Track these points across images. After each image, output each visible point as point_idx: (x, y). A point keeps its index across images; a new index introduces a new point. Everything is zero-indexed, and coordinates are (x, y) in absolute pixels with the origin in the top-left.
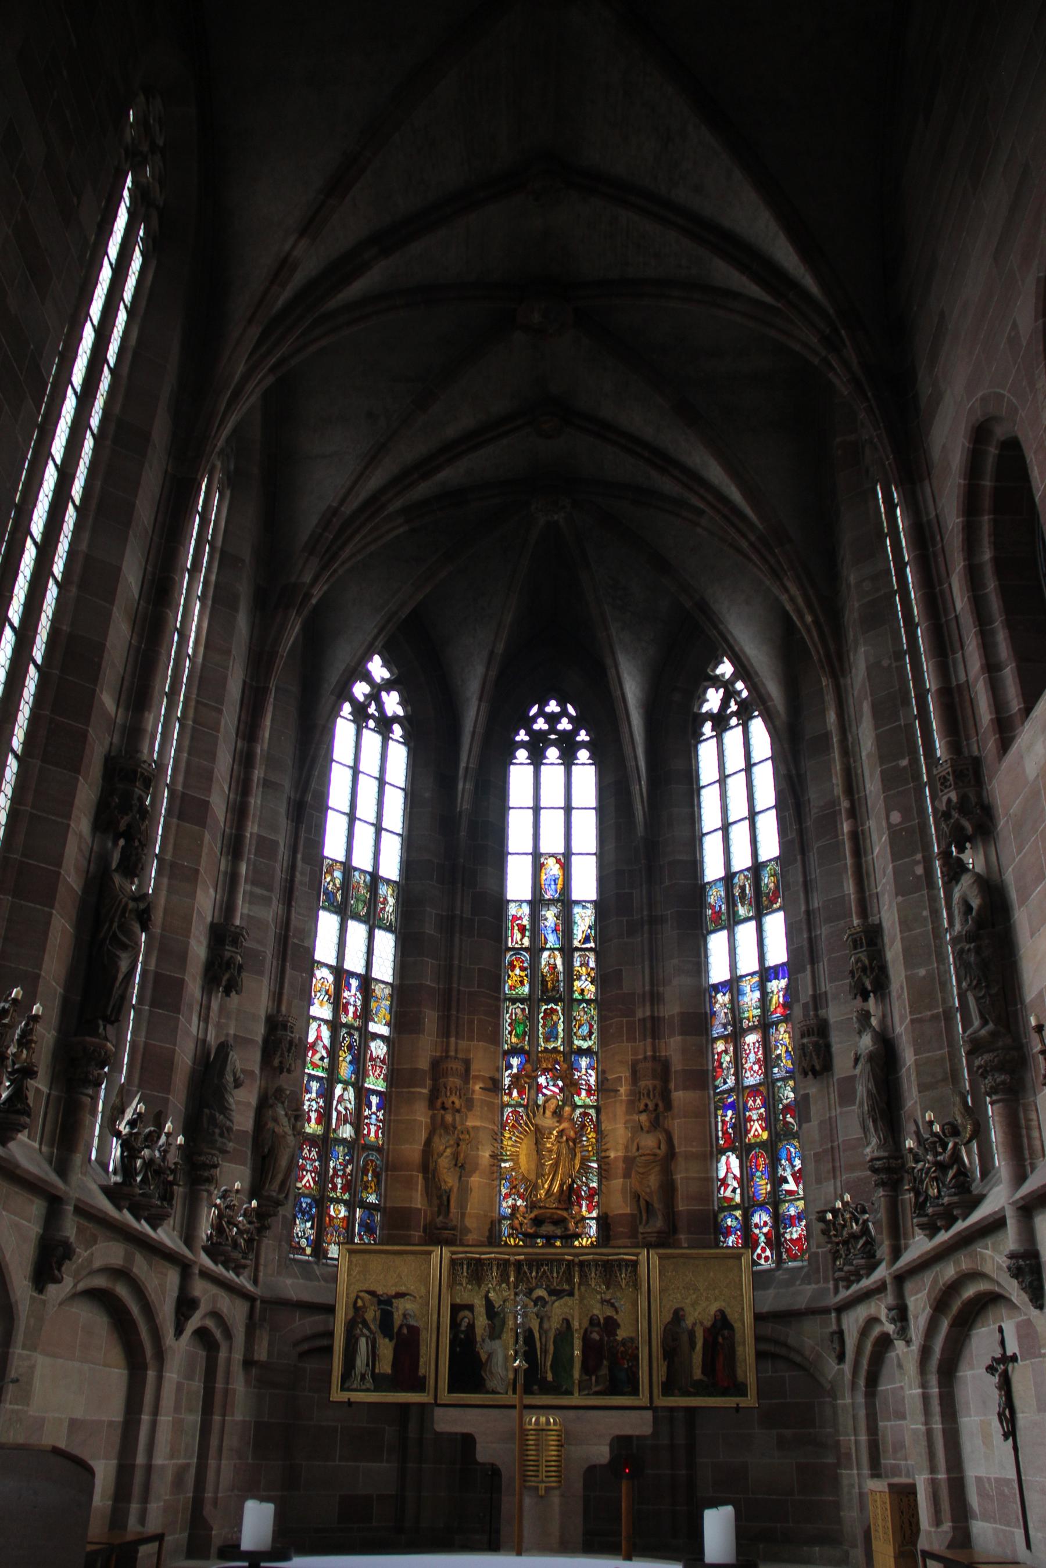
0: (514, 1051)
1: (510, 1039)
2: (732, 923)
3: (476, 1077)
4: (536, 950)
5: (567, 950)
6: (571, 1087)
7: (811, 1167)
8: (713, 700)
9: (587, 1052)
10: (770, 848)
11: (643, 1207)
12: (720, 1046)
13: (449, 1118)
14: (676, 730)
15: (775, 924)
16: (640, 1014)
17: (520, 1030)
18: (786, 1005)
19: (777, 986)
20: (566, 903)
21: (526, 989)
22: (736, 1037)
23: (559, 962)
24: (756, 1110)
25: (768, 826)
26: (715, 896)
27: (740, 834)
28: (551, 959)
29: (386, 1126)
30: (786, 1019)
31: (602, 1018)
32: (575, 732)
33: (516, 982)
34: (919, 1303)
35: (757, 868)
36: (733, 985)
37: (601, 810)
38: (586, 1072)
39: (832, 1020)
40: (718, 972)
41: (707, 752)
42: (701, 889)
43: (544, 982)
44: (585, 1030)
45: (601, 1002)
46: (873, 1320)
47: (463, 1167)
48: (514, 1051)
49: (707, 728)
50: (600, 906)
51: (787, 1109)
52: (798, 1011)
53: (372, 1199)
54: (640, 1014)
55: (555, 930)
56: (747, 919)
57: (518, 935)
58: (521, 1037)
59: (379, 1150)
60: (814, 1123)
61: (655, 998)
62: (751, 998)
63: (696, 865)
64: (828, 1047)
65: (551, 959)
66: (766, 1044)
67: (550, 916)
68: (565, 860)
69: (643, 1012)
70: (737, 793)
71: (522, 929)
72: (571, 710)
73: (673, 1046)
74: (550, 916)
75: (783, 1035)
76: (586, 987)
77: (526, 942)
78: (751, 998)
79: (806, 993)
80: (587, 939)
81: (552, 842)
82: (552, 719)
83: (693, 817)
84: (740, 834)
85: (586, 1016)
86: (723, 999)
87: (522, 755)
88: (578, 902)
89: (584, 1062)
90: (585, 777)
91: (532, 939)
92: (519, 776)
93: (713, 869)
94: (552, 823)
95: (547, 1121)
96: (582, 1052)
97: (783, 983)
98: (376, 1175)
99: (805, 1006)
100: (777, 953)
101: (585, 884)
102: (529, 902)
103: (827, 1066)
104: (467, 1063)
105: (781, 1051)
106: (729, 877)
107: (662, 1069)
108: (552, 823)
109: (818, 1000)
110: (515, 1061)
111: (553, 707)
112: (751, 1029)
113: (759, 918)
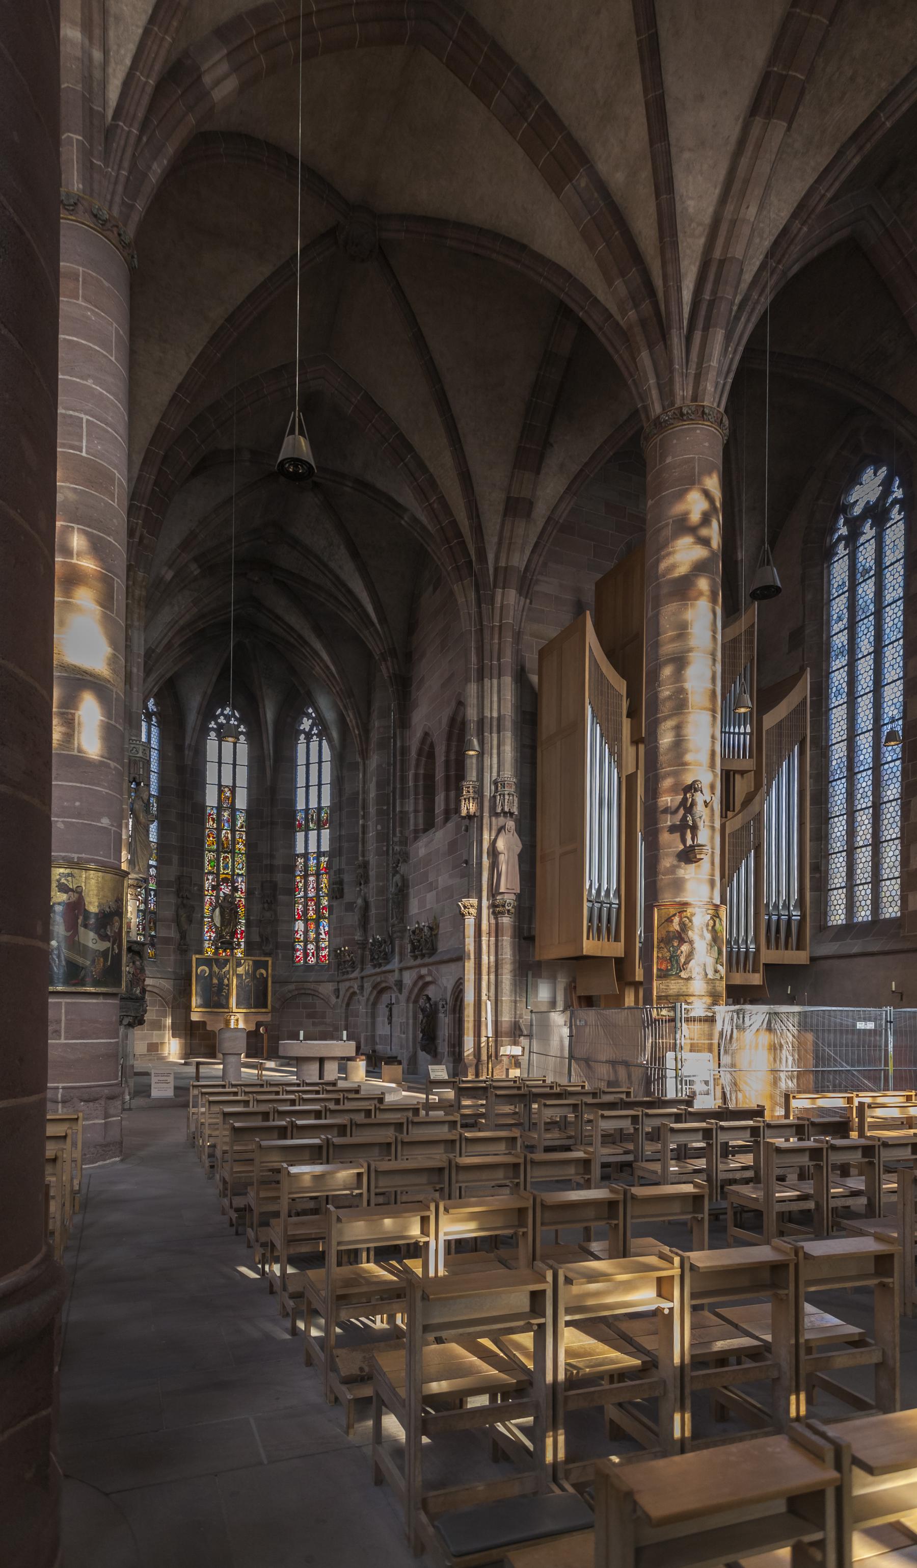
0: (210, 873)
1: (208, 868)
2: (307, 830)
3: (195, 884)
4: (219, 830)
5: (233, 831)
6: (235, 889)
7: (332, 931)
8: (306, 724)
9: (242, 875)
10: (326, 802)
11: (265, 939)
12: (298, 879)
13: (185, 902)
14: (286, 734)
15: (326, 833)
16: (264, 862)
17: (212, 864)
18: (326, 868)
19: (324, 860)
20: (233, 810)
21: (215, 847)
22: (306, 877)
23: (229, 836)
24: (312, 906)
25: (326, 790)
26: (300, 816)
27: (313, 791)
28: (226, 833)
29: (157, 903)
30: (326, 873)
31: (248, 862)
32: (238, 726)
33: (210, 842)
34: (368, 986)
35: (320, 809)
36: (306, 856)
37: (250, 767)
38: (241, 884)
39: (346, 880)
40: (300, 849)
41: (301, 748)
42: (294, 813)
43: (223, 844)
44: (241, 866)
45: (248, 855)
46: (350, 987)
47: (190, 920)
48: (210, 873)
49: (302, 736)
50: (249, 813)
51: (324, 908)
52: (332, 872)
53: (153, 933)
54: (264, 862)
55: (228, 821)
56: (313, 830)
57: (211, 823)
58: (213, 867)
59: (155, 913)
60: (334, 916)
61: (272, 856)
62: (312, 863)
63: (292, 802)
64: (343, 889)
65: (226, 833)
66: (318, 882)
67: (226, 814)
68: (233, 790)
69: (266, 862)
70: (314, 775)
71: (213, 820)
72: (237, 714)
73: (279, 877)
74: (226, 814)
75: (325, 880)
76: (240, 846)
77: (215, 826)
78: (312, 863)
79: (336, 867)
80: (242, 827)
81: (227, 781)
82: (228, 718)
83: (293, 780)
84: (313, 791)
85: (241, 860)
86: (301, 860)
87: (213, 734)
88: (238, 810)
89: (240, 879)
90: (243, 748)
91: (219, 823)
92: (212, 744)
93: (301, 805)
94: (227, 770)
95: (226, 905)
96: (238, 875)
97: (326, 859)
98: (155, 924)
99: (335, 872)
100: (325, 847)
101: (241, 803)
102: (217, 808)
103: (342, 897)
104: (191, 878)
105: (323, 885)
106: (307, 810)
107: (274, 886)
108: (227, 770)
109: (340, 871)
110: (210, 877)
111: (227, 711)
112: (312, 875)
113: (319, 828)
